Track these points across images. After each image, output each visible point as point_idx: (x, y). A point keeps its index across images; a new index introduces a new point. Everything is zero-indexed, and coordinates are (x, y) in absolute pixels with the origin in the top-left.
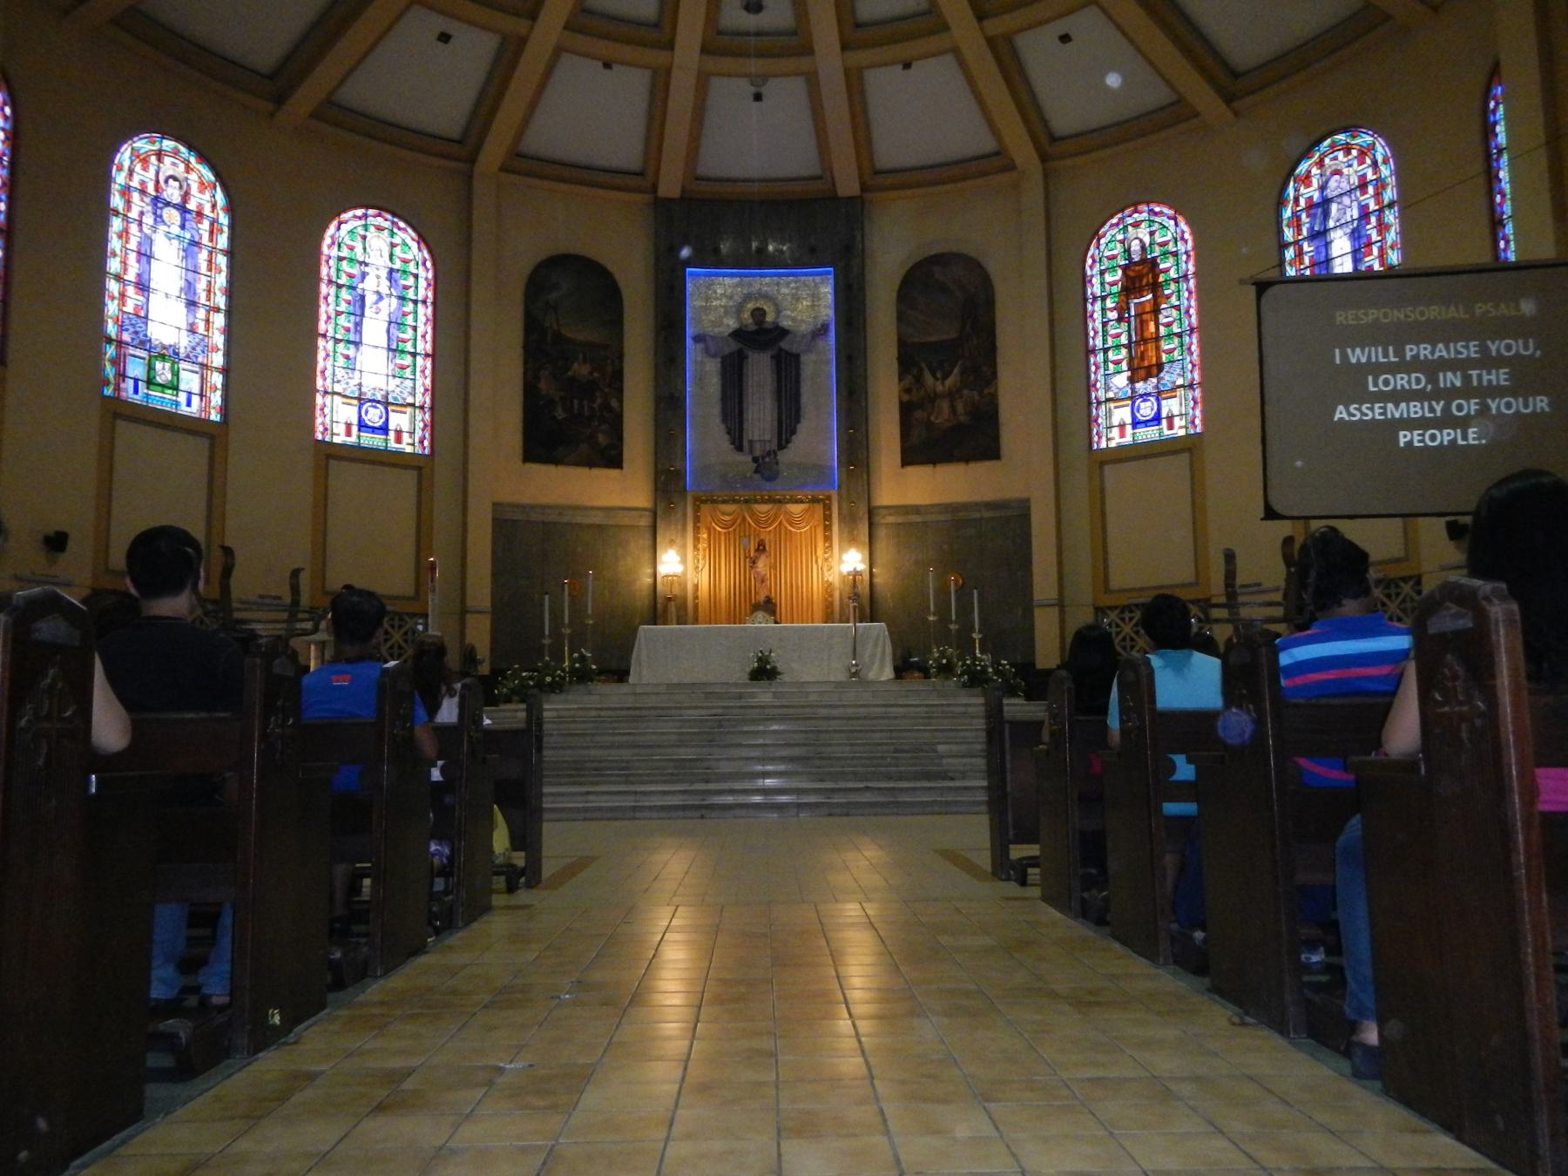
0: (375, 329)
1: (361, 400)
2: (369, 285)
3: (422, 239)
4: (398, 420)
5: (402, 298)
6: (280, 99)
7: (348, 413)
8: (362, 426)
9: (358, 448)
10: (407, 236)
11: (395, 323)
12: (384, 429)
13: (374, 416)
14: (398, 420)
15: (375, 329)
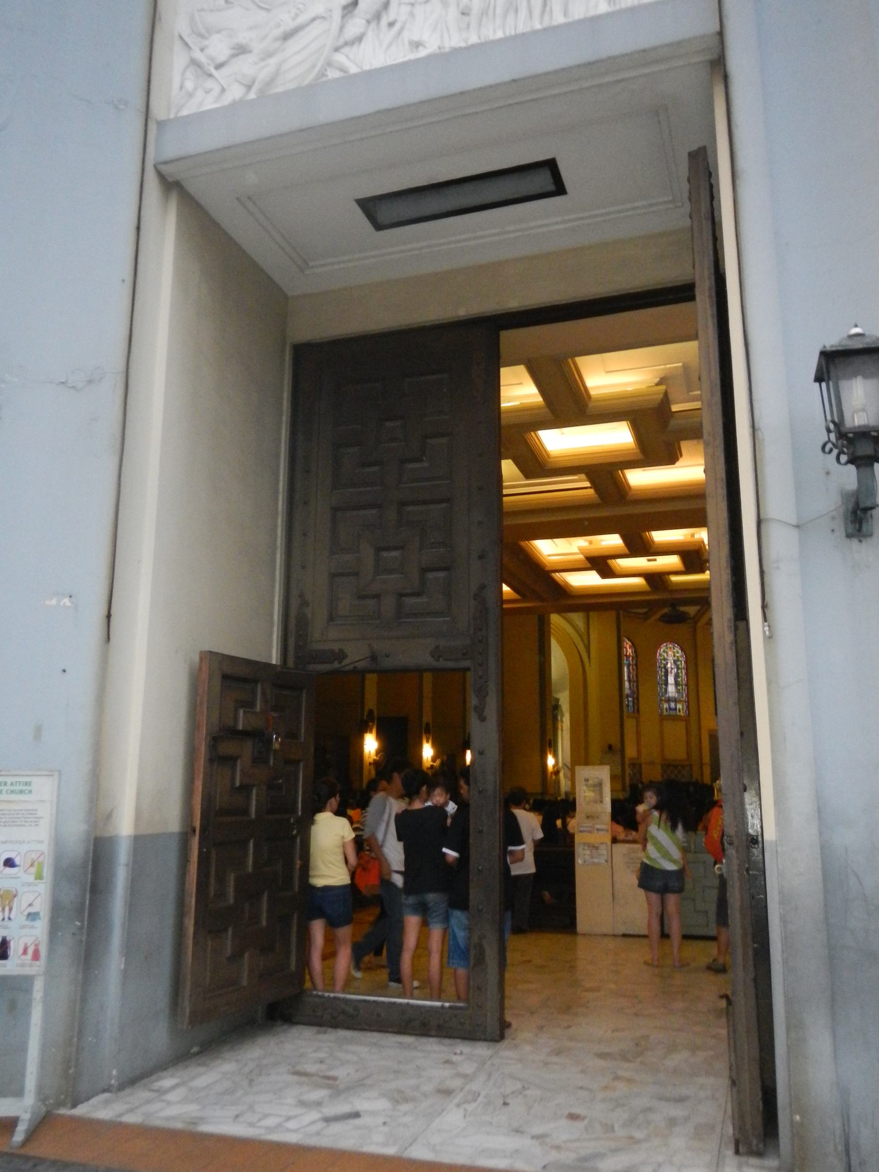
0: (671, 680)
1: (669, 700)
2: (669, 665)
3: (682, 650)
4: (679, 706)
5: (678, 668)
6: (646, 619)
7: (666, 706)
8: (670, 709)
9: (669, 715)
10: (677, 649)
11: (677, 676)
12: (676, 709)
13: (673, 705)
14: (679, 706)
15: (671, 680)
